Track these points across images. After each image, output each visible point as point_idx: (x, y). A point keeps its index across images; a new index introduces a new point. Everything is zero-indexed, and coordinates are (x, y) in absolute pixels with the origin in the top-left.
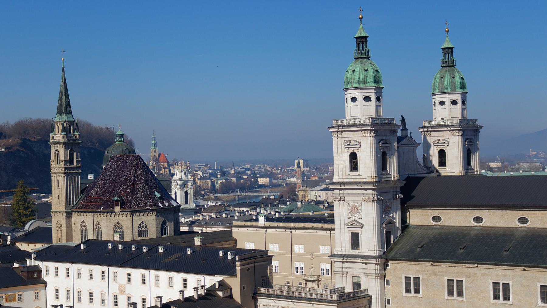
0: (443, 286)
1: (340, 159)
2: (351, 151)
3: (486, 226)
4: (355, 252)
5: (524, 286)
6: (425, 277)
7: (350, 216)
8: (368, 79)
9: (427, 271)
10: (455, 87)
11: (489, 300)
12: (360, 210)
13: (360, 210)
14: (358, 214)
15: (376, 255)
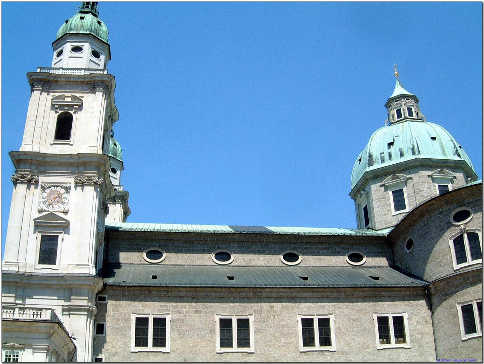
0: (213, 331)
1: (39, 120)
2: (60, 112)
3: (236, 264)
4: (46, 269)
5: (353, 320)
6: (177, 316)
7: (44, 208)
8: (100, 32)
9: (180, 307)
10: (116, 155)
11: (297, 347)
12: (66, 198)
13: (66, 198)
14: (60, 204)
15: (91, 273)
